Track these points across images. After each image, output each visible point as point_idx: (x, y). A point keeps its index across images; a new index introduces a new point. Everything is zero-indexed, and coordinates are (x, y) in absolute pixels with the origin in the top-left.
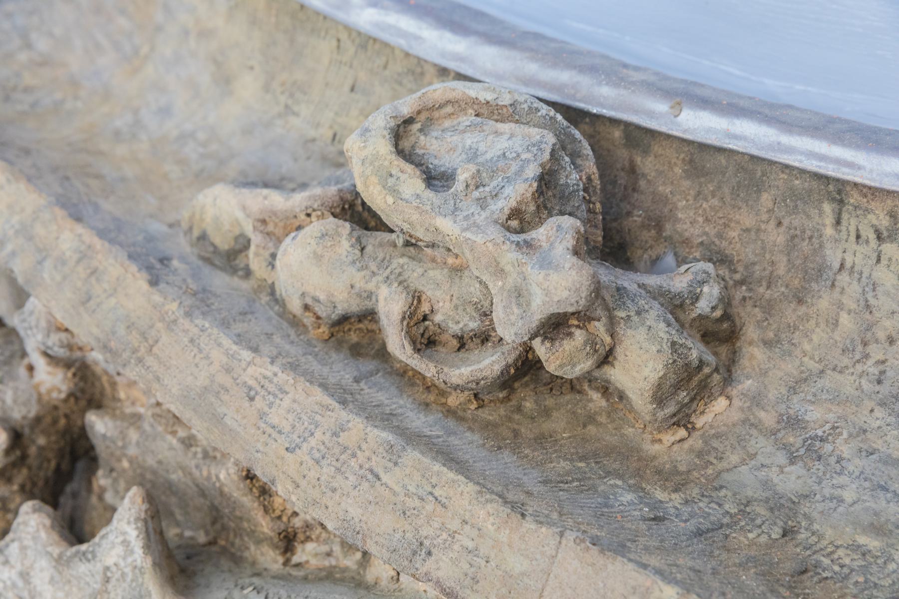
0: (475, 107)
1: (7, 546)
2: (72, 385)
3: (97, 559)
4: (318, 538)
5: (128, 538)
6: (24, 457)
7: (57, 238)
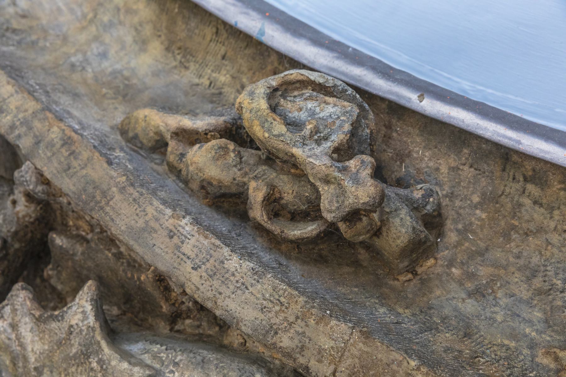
0: (313, 85)
1: (3, 307)
2: (39, 214)
3: (65, 320)
4: (195, 316)
5: (86, 310)
6: (7, 255)
7: (49, 130)
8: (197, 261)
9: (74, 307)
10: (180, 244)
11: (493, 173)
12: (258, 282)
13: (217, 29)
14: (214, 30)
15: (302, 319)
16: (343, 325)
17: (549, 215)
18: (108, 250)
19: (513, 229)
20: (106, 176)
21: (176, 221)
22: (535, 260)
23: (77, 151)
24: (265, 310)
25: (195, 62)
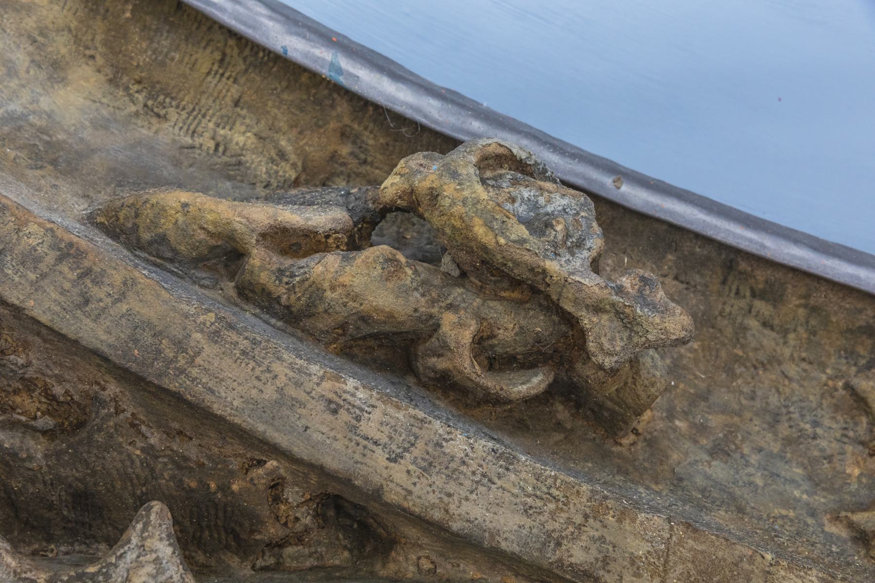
5: (161, 555)
7: (18, 231)
8: (394, 447)
9: (129, 553)
10: (354, 422)
11: (707, 286)
12: (507, 469)
13: (224, 55)
14: (217, 56)
15: (595, 518)
16: (656, 518)
17: (782, 340)
18: (130, 444)
19: (737, 361)
20: (172, 314)
21: (337, 384)
22: (774, 400)
23: (97, 269)
24: (531, 512)
25: (177, 107)
